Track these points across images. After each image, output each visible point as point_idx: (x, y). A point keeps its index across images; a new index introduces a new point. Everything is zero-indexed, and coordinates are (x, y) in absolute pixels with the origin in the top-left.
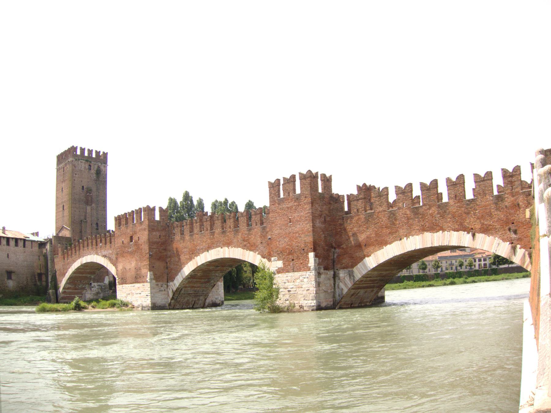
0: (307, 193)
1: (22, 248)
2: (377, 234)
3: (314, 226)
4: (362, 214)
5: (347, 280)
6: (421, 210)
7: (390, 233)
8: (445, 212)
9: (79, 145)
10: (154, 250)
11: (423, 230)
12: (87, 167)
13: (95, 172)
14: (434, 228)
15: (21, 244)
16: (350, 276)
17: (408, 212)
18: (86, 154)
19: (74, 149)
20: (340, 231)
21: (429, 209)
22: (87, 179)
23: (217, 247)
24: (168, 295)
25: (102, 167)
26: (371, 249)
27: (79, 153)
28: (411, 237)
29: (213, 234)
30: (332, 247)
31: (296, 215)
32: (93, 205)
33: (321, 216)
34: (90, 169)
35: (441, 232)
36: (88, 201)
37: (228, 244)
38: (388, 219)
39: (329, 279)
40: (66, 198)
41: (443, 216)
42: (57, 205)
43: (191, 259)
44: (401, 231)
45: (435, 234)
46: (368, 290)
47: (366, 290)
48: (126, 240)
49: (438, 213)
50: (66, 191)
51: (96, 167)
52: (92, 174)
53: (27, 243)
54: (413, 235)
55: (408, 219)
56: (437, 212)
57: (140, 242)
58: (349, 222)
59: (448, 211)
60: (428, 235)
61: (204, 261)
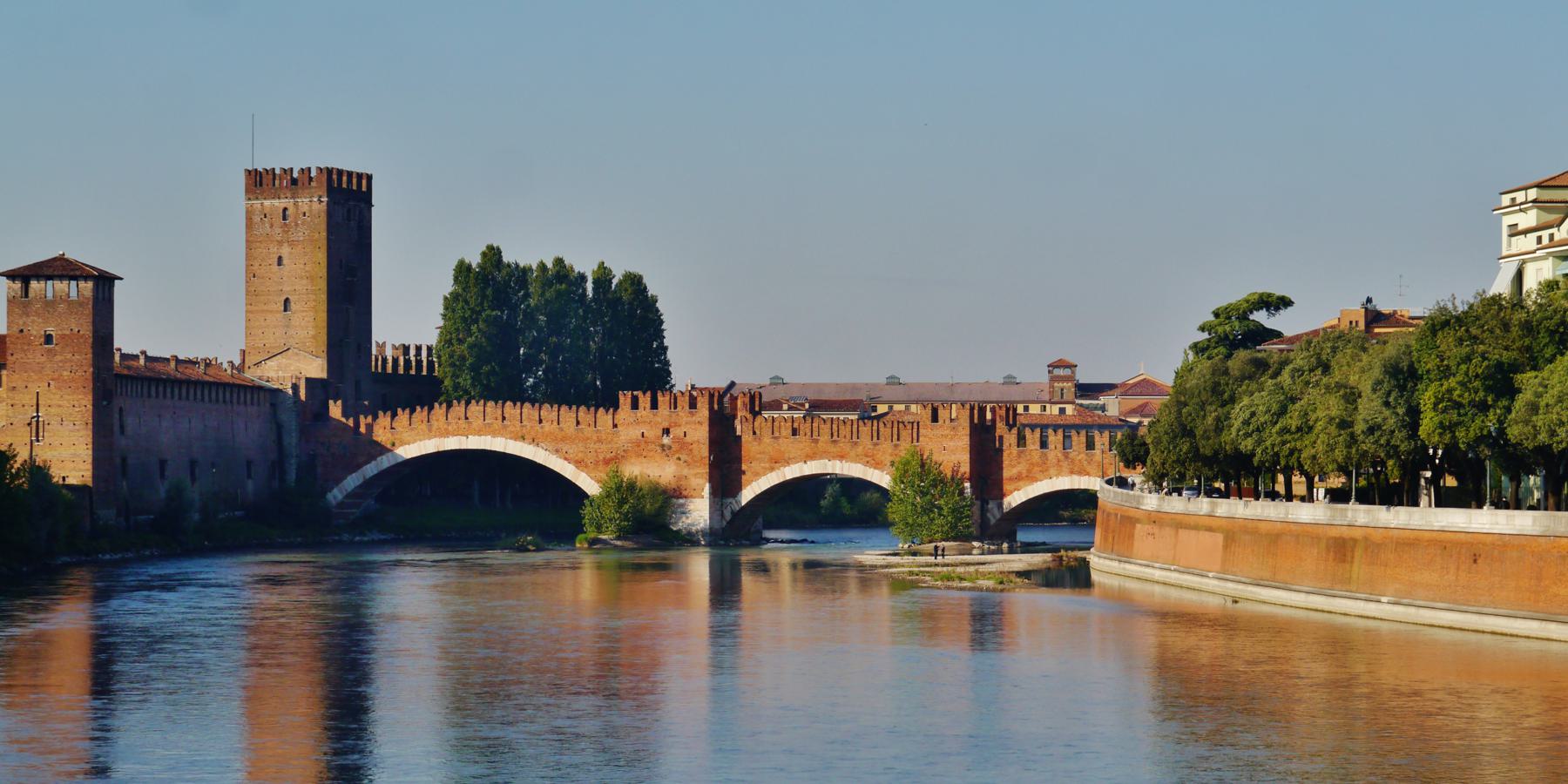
0: (967, 424)
11: (1072, 472)
14: (1082, 472)
23: (821, 458)
24: (722, 515)
29: (816, 441)
37: (842, 457)
42: (252, 294)
43: (772, 469)
44: (1052, 471)
48: (652, 433)
57: (688, 439)
60: (1075, 477)
61: (798, 475)
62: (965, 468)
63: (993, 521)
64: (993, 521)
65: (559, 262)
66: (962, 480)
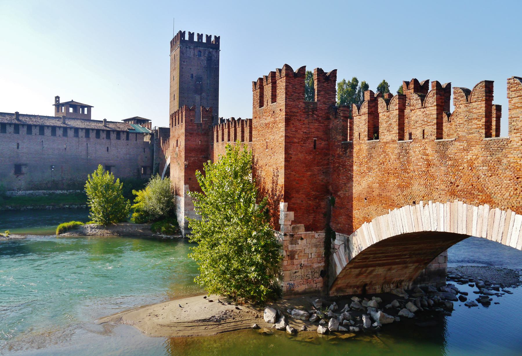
1: (125, 141)
2: (381, 184)
3: (287, 160)
4: (365, 144)
5: (342, 250)
6: (452, 150)
7: (399, 186)
8: (499, 161)
9: (187, 29)
10: (192, 159)
11: (454, 193)
12: (196, 53)
13: (205, 58)
15: (123, 136)
16: (345, 247)
17: (429, 151)
18: (196, 39)
19: (182, 34)
20: (338, 167)
21: (466, 150)
22: (197, 68)
25: (214, 53)
26: (372, 208)
27: (187, 38)
28: (430, 202)
30: (328, 192)
31: (272, 137)
32: (204, 94)
33: (305, 140)
35: (487, 206)
36: (199, 90)
38: (399, 158)
39: (316, 246)
40: (176, 87)
41: (493, 171)
44: (417, 188)
45: (475, 208)
46: (394, 267)
47: (389, 267)
49: (484, 163)
50: (177, 79)
51: (207, 53)
53: (130, 135)
54: (434, 201)
55: (429, 165)
56: (481, 159)
58: (348, 154)
59: (505, 161)
60: (460, 206)
62: (281, 181)
63: (339, 270)
64: (339, 270)
65: (355, 80)
66: (277, 203)
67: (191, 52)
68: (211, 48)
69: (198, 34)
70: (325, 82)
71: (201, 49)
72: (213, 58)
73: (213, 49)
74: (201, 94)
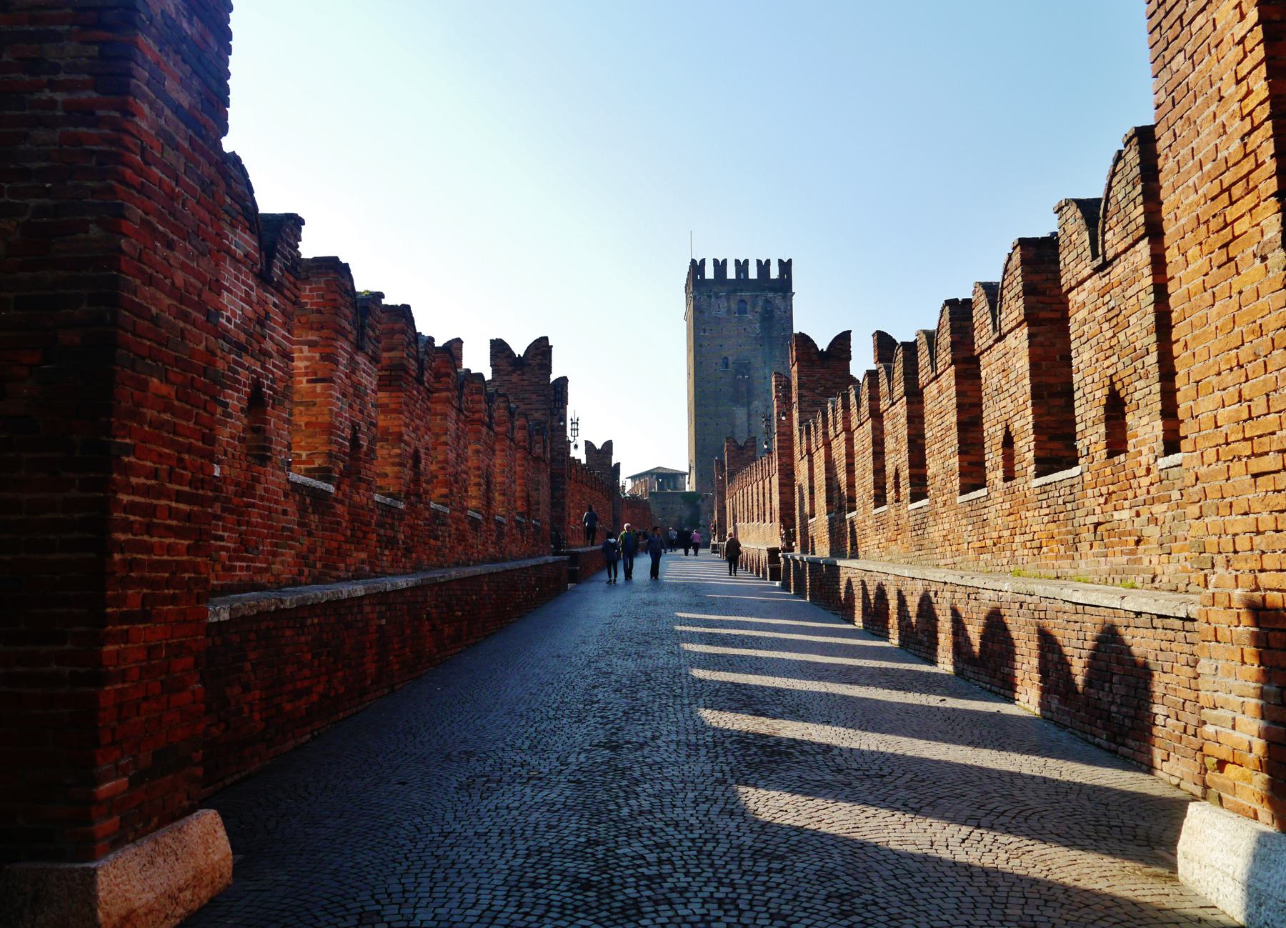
9: (709, 255)
12: (734, 306)
25: (778, 301)
27: (709, 273)
34: (742, 311)
51: (760, 303)
52: (750, 322)
67: (721, 307)
68: (771, 290)
69: (737, 262)
70: (514, 371)
71: (746, 294)
72: (777, 313)
73: (775, 290)
74: (749, 404)
